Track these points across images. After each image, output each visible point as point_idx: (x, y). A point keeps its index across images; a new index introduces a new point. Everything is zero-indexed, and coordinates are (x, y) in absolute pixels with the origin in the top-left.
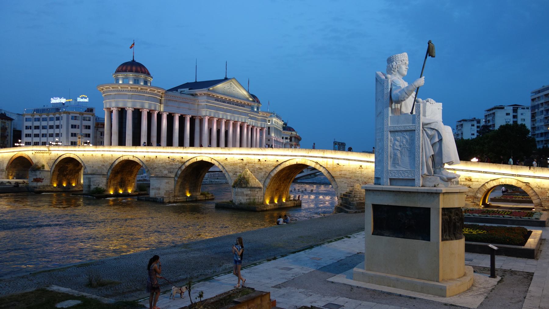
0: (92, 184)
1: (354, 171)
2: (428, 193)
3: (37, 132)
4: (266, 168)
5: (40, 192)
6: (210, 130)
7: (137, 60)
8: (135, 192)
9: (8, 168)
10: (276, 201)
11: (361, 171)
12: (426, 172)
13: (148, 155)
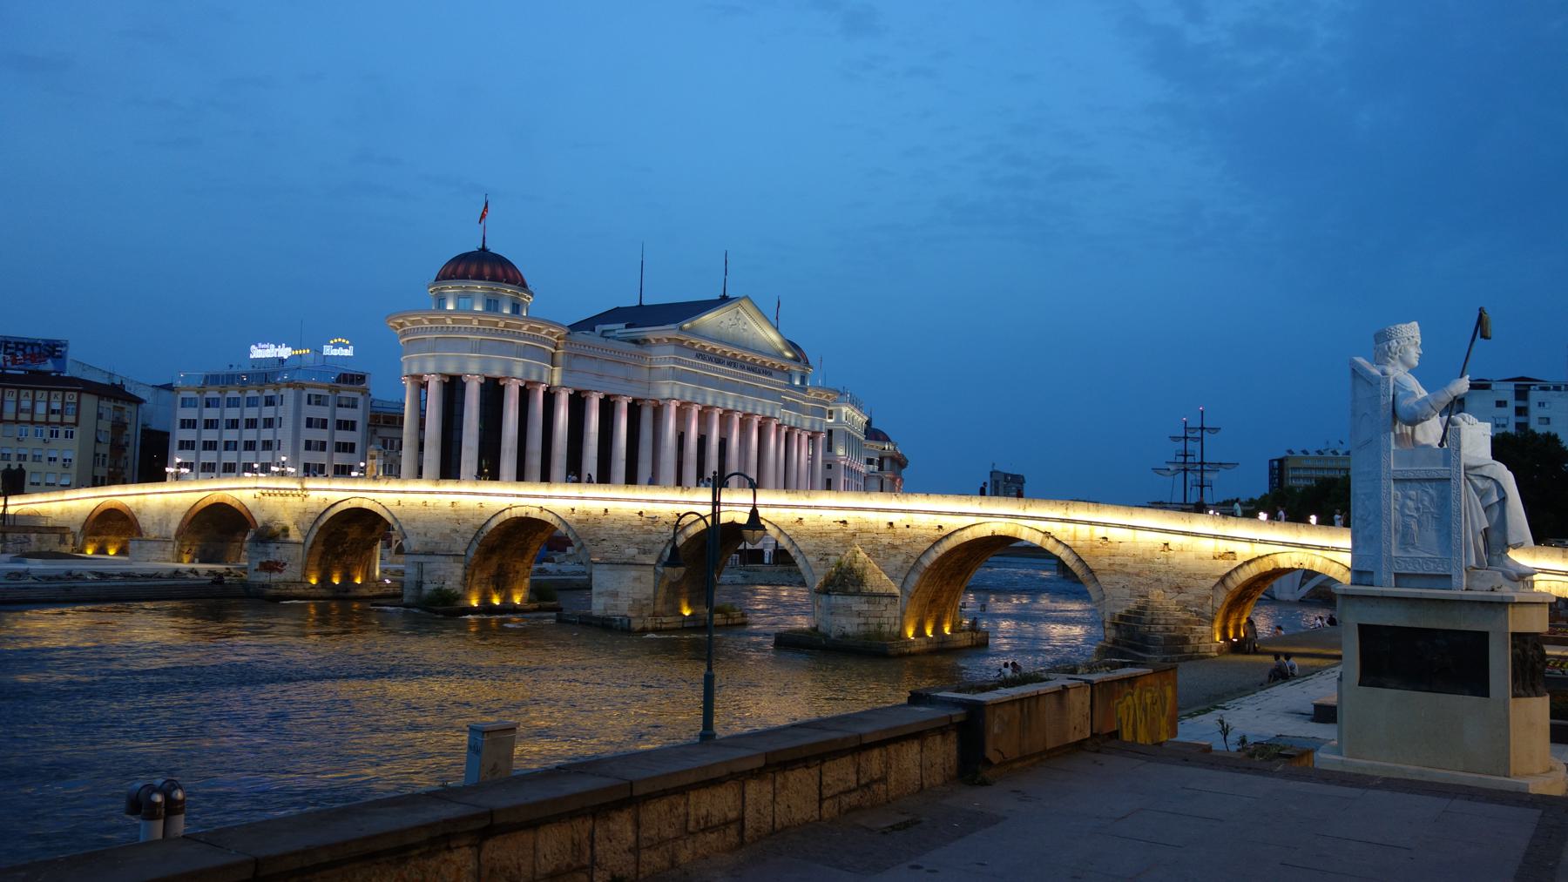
0: (426, 579)
1: (1148, 556)
2: (1482, 603)
3: (210, 435)
4: (908, 544)
5: (277, 599)
6: (681, 438)
7: (494, 247)
8: (530, 601)
9: (180, 533)
10: (929, 632)
11: (1167, 557)
12: (1473, 562)
13: (580, 505)
